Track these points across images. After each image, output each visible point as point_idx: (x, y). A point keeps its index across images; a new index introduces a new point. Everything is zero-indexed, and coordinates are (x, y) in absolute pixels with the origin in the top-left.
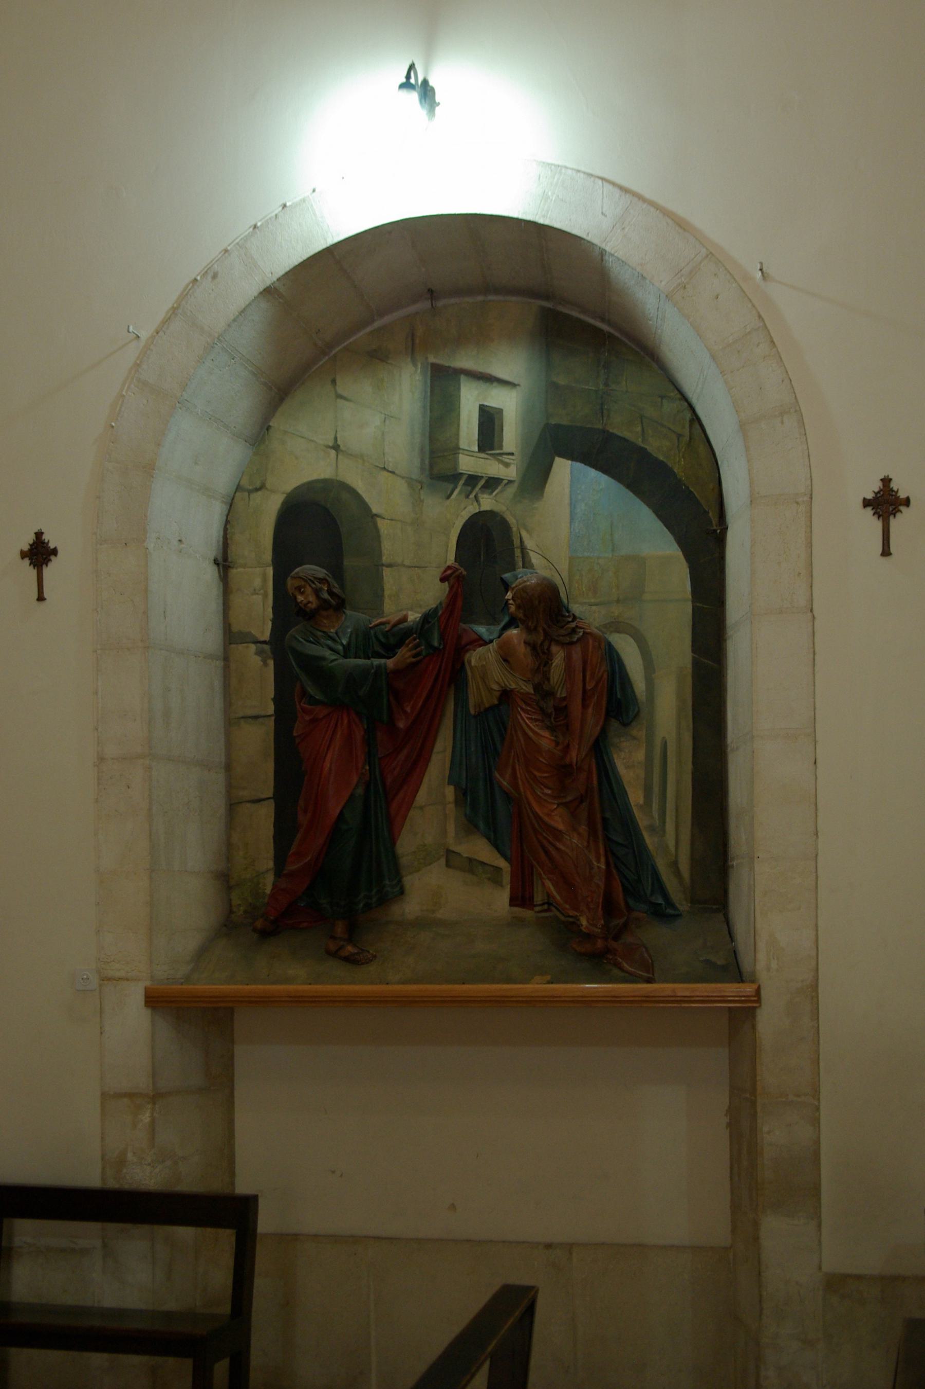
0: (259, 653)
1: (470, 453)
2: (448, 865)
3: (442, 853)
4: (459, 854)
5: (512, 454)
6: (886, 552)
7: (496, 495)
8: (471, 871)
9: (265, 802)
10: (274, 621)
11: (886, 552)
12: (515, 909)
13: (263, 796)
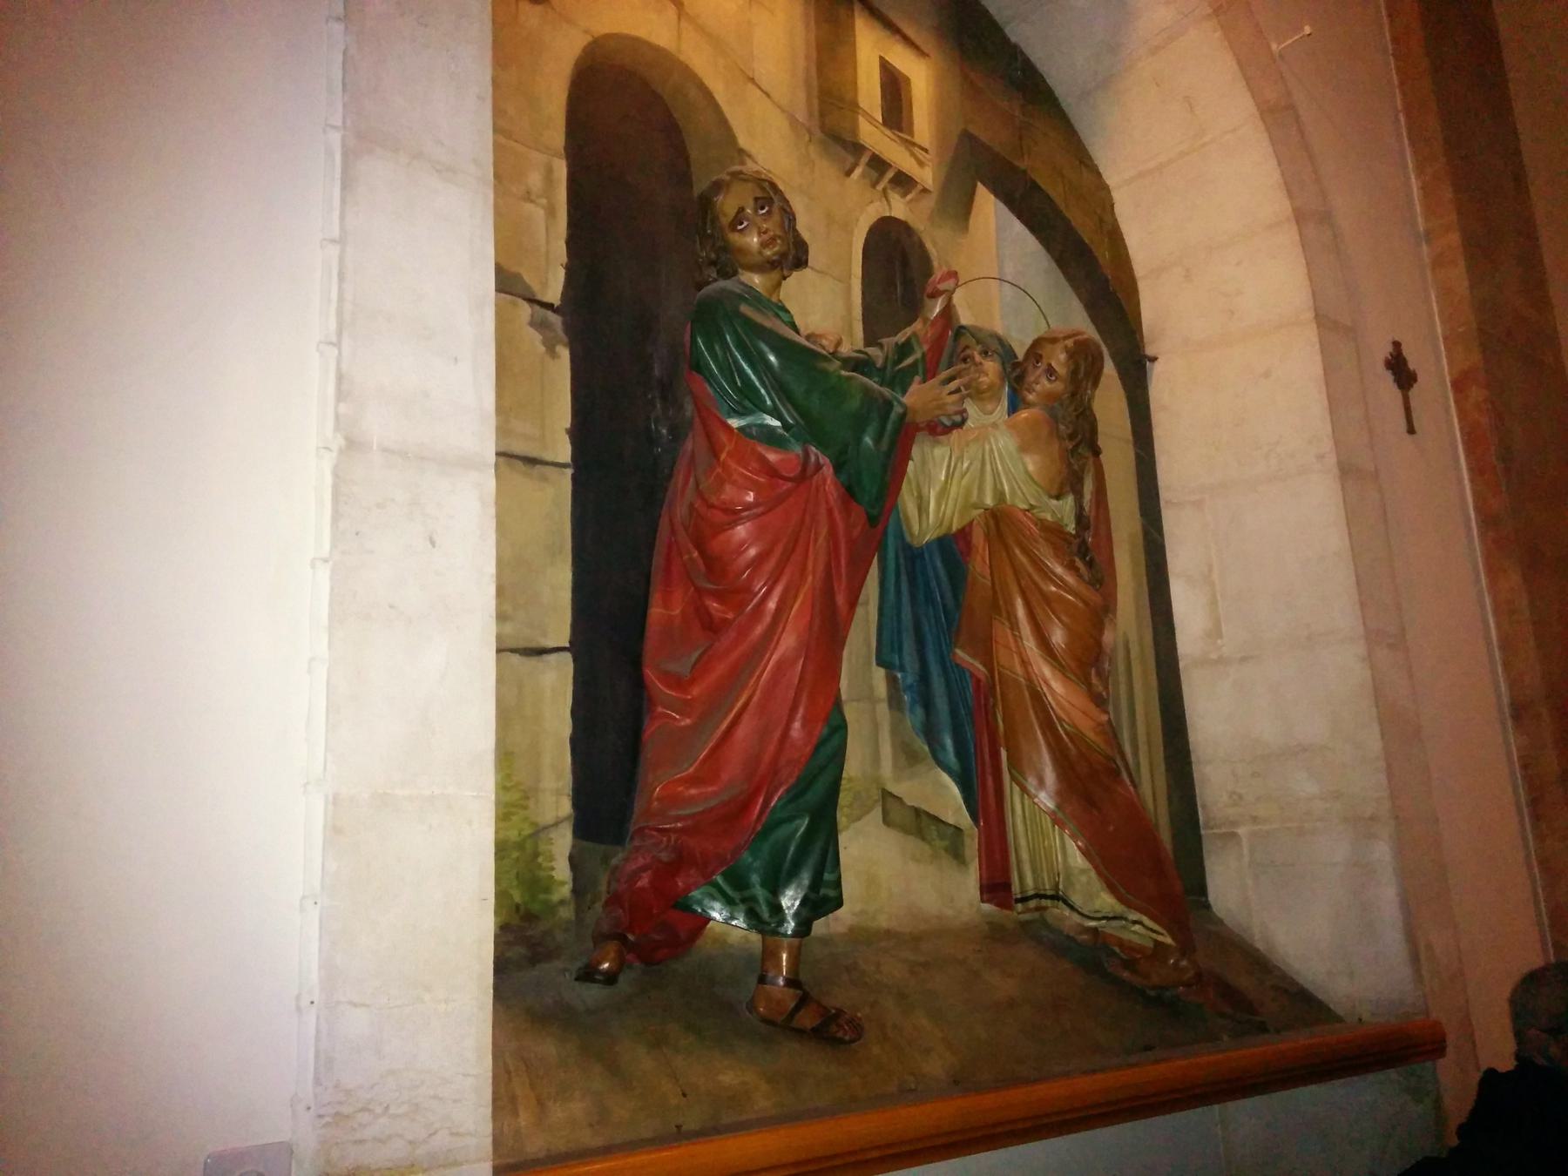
0: (539, 325)
1: (871, 119)
2: (887, 821)
3: (876, 798)
4: (899, 799)
5: (926, 151)
6: (1411, 430)
7: (911, 201)
8: (920, 834)
9: (553, 657)
10: (570, 271)
11: (1411, 430)
12: (987, 907)
13: (551, 644)
